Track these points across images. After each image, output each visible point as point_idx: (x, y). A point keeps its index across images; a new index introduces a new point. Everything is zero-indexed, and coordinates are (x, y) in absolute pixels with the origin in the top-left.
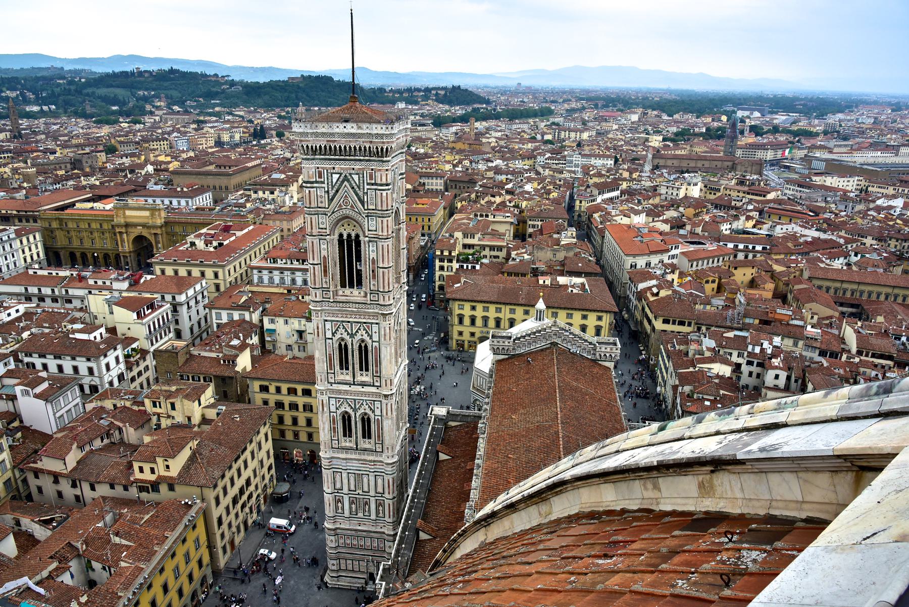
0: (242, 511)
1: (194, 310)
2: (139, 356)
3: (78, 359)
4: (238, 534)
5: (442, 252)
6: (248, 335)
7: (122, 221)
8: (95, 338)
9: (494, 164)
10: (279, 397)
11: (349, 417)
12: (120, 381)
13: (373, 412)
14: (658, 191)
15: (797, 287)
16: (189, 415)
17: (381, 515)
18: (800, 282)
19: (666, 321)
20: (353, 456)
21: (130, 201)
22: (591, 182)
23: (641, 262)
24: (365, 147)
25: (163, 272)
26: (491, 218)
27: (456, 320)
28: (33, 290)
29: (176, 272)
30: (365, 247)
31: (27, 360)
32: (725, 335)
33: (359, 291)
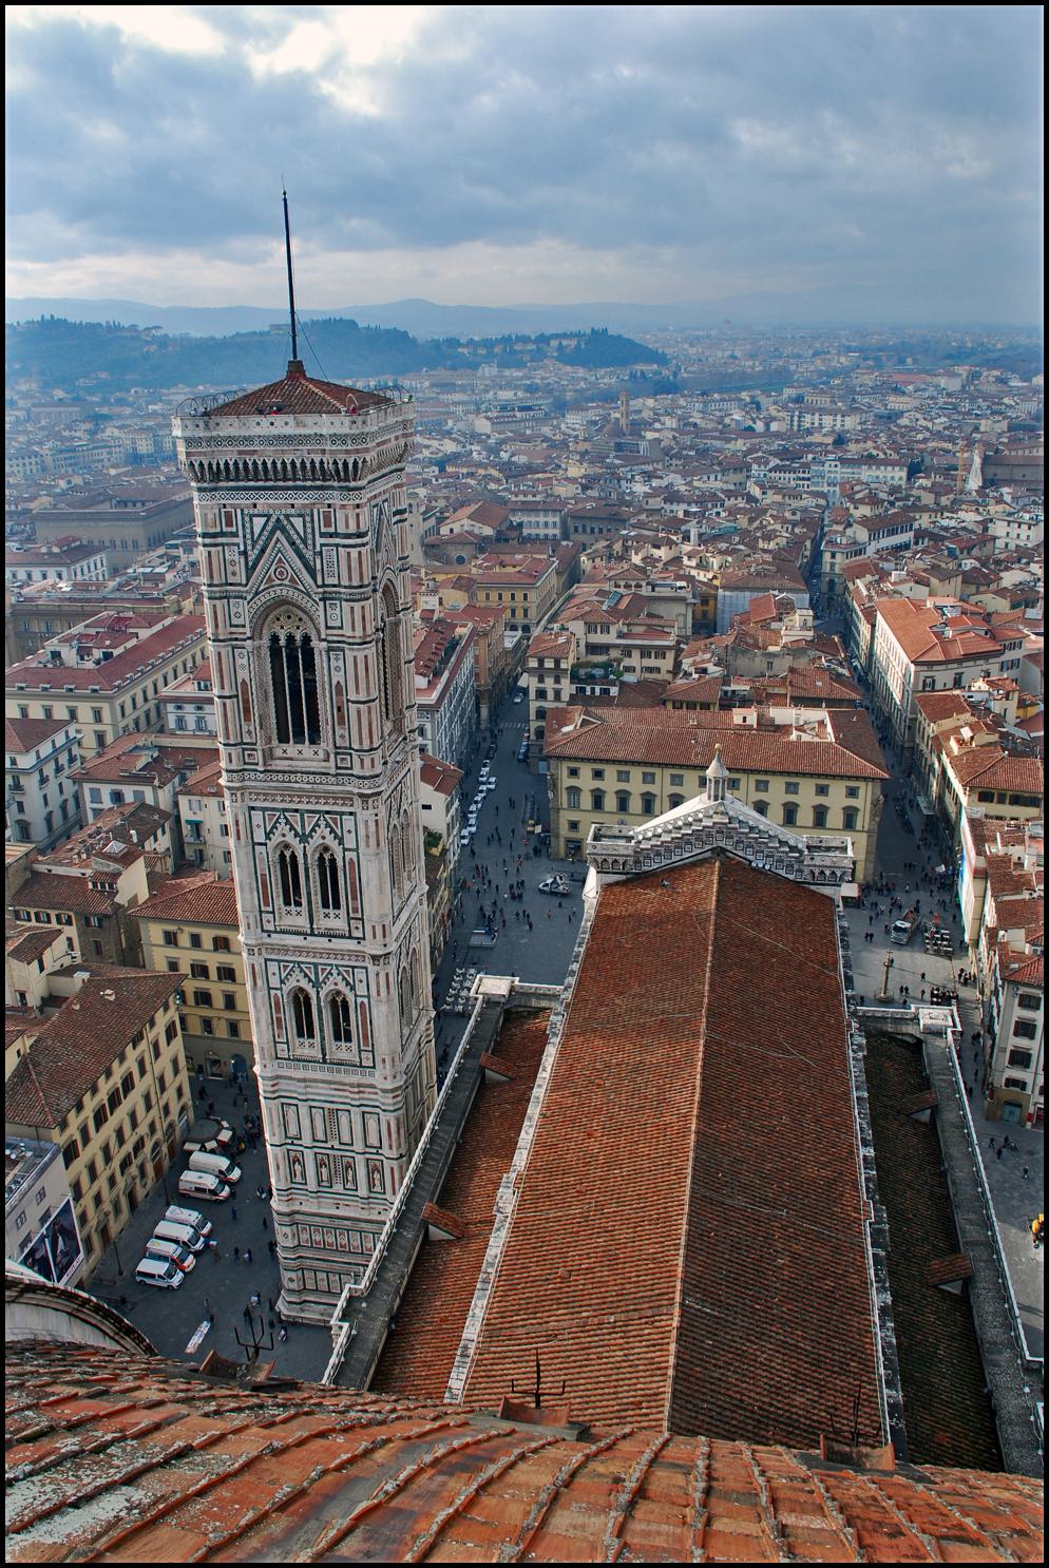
0: (123, 1174)
1: (52, 788)
4: (116, 1217)
5: (541, 662)
6: (148, 832)
9: (664, 483)
10: (198, 956)
11: (307, 999)
13: (353, 988)
14: (990, 532)
17: (378, 1188)
24: (313, 462)
26: (646, 591)
27: (564, 799)
33: (314, 748)
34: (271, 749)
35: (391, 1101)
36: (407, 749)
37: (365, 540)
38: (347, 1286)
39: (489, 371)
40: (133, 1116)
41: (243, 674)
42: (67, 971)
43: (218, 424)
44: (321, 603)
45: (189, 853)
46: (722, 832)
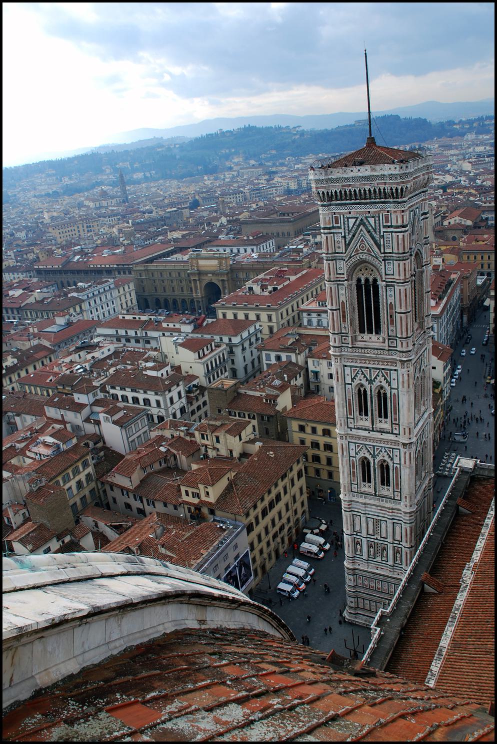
0: (273, 541)
1: (247, 353)
2: (198, 392)
3: (148, 392)
8: (162, 375)
11: (369, 463)
12: (181, 414)
13: (392, 459)
16: (231, 448)
17: (398, 562)
24: (380, 189)
25: (224, 315)
28: (122, 332)
29: (235, 316)
30: (383, 291)
31: (112, 391)
33: (378, 336)
34: (355, 336)
35: (408, 518)
36: (426, 337)
37: (406, 229)
38: (381, 610)
39: (470, 137)
40: (280, 513)
41: (343, 298)
42: (252, 442)
43: (331, 172)
44: (383, 262)
45: (312, 387)
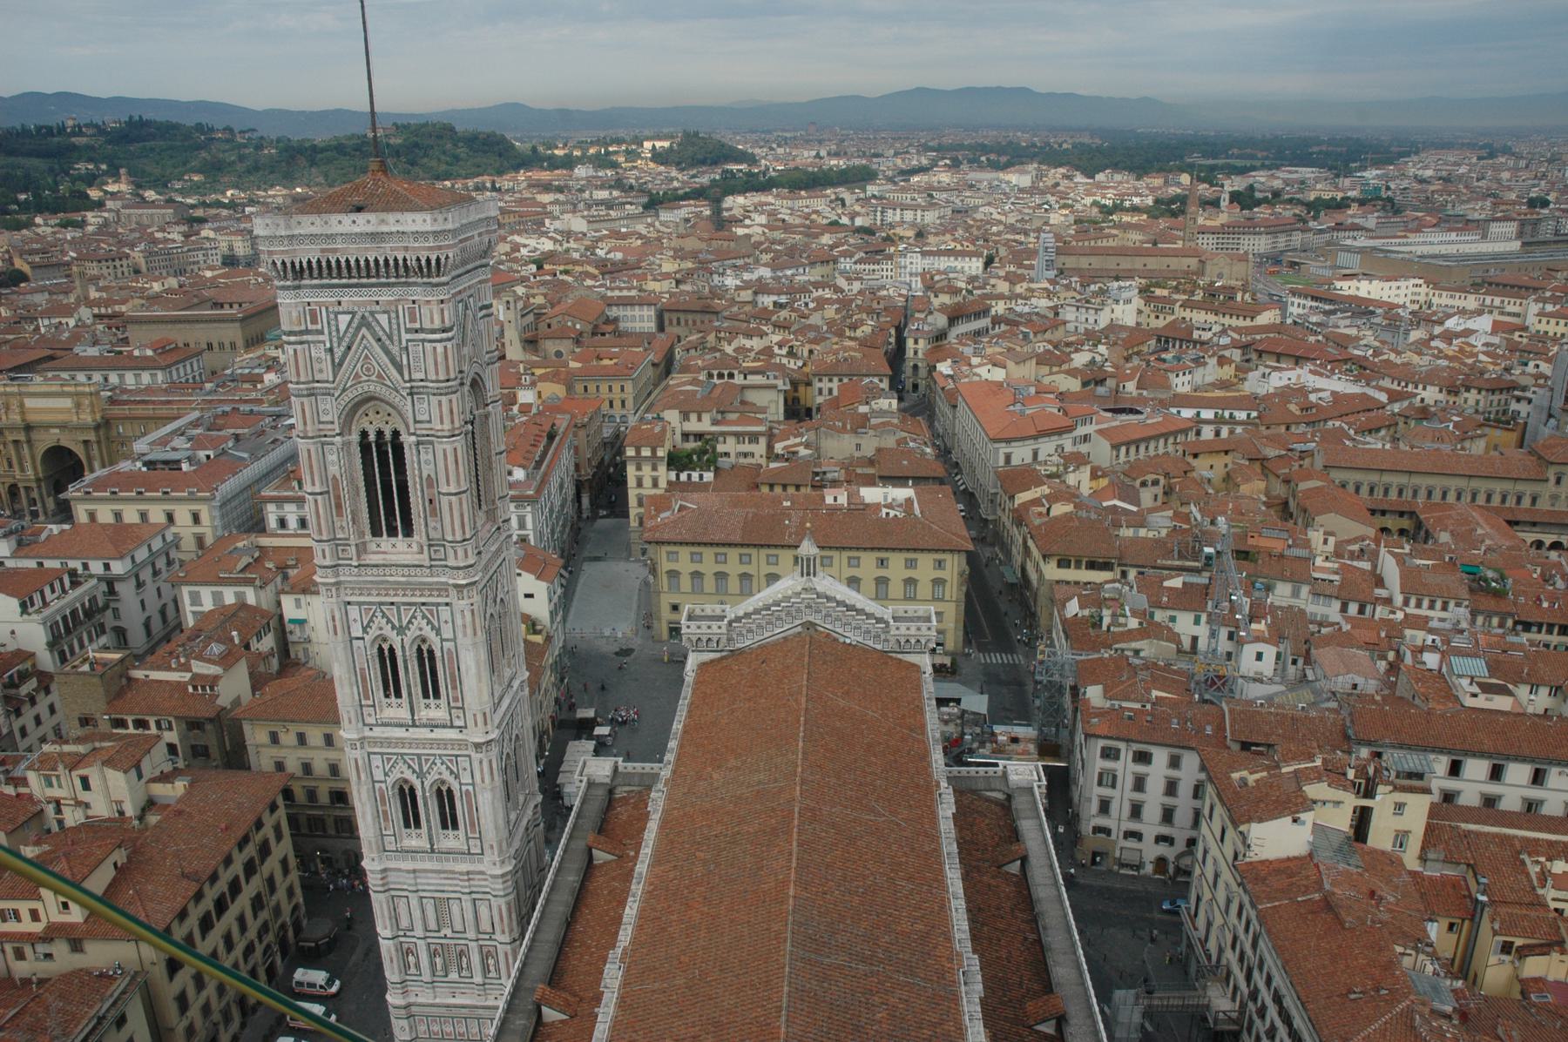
1: (150, 588)
5: (638, 451)
7: (16, 418)
9: (754, 276)
10: (304, 754)
11: (412, 790)
13: (457, 777)
14: (1061, 317)
15: (1303, 486)
17: (493, 974)
18: (1309, 477)
19: (1063, 563)
20: (428, 865)
21: (38, 379)
22: (936, 302)
23: (1021, 454)
24: (396, 260)
25: (92, 516)
26: (738, 380)
29: (118, 515)
32: (1167, 584)
34: (364, 544)
35: (501, 886)
37: (450, 334)
41: (334, 470)
43: (299, 223)
44: (409, 398)
46: (811, 607)
